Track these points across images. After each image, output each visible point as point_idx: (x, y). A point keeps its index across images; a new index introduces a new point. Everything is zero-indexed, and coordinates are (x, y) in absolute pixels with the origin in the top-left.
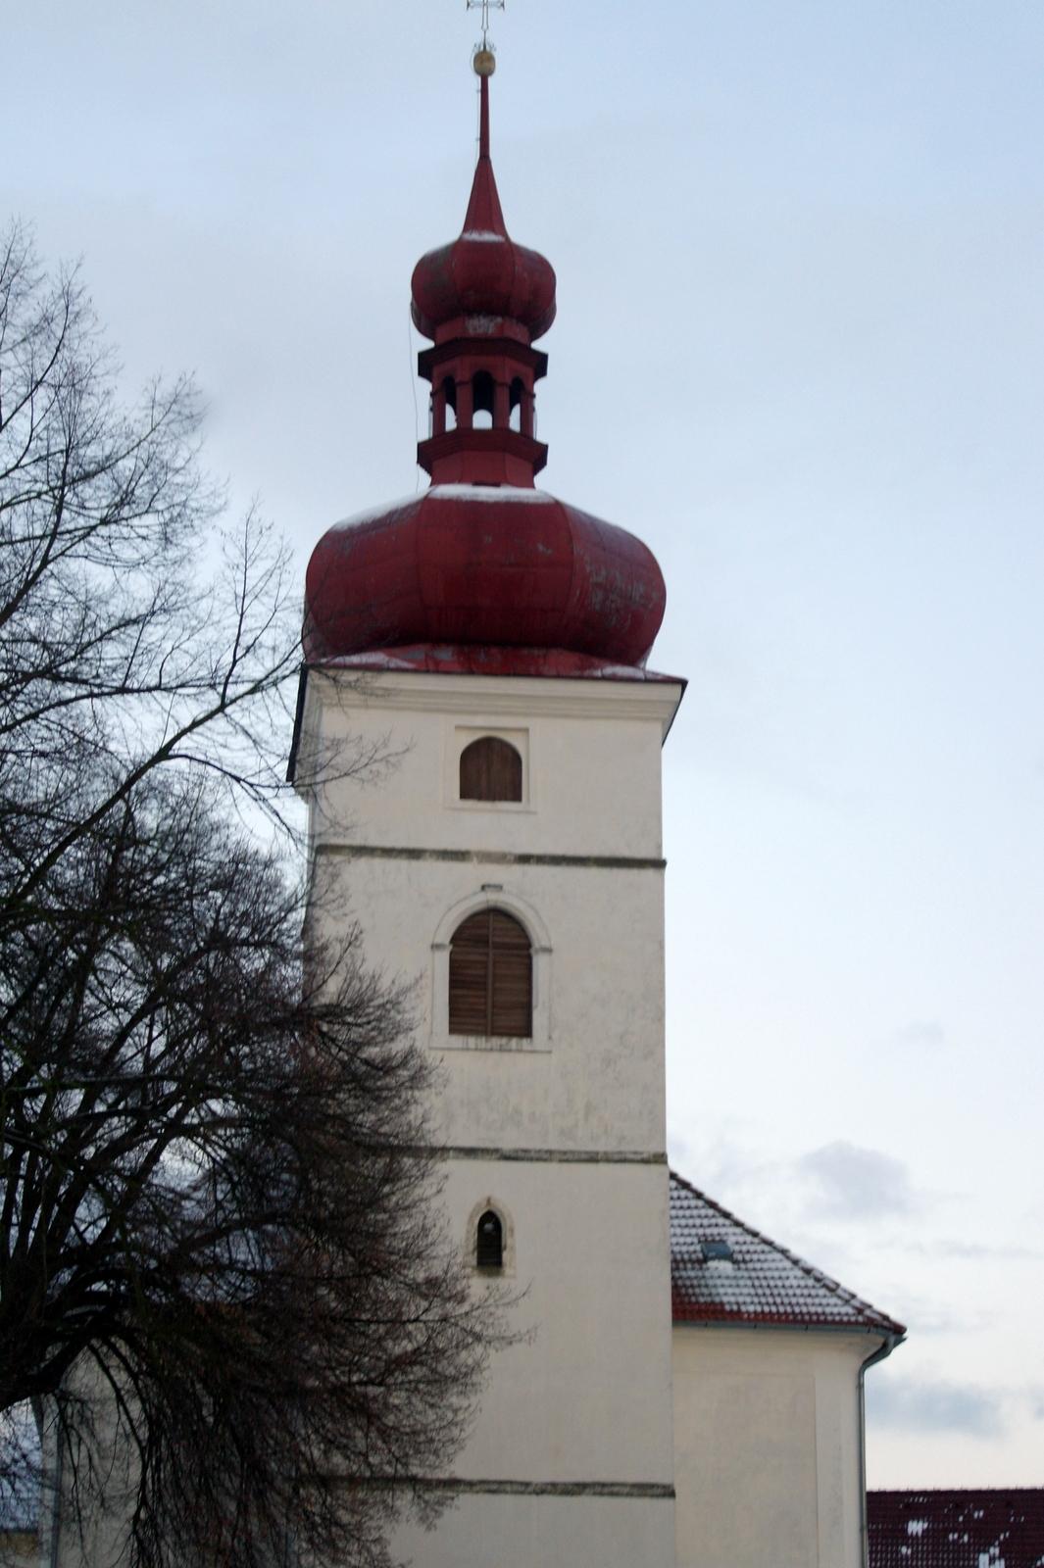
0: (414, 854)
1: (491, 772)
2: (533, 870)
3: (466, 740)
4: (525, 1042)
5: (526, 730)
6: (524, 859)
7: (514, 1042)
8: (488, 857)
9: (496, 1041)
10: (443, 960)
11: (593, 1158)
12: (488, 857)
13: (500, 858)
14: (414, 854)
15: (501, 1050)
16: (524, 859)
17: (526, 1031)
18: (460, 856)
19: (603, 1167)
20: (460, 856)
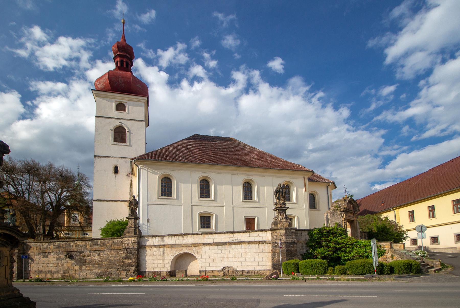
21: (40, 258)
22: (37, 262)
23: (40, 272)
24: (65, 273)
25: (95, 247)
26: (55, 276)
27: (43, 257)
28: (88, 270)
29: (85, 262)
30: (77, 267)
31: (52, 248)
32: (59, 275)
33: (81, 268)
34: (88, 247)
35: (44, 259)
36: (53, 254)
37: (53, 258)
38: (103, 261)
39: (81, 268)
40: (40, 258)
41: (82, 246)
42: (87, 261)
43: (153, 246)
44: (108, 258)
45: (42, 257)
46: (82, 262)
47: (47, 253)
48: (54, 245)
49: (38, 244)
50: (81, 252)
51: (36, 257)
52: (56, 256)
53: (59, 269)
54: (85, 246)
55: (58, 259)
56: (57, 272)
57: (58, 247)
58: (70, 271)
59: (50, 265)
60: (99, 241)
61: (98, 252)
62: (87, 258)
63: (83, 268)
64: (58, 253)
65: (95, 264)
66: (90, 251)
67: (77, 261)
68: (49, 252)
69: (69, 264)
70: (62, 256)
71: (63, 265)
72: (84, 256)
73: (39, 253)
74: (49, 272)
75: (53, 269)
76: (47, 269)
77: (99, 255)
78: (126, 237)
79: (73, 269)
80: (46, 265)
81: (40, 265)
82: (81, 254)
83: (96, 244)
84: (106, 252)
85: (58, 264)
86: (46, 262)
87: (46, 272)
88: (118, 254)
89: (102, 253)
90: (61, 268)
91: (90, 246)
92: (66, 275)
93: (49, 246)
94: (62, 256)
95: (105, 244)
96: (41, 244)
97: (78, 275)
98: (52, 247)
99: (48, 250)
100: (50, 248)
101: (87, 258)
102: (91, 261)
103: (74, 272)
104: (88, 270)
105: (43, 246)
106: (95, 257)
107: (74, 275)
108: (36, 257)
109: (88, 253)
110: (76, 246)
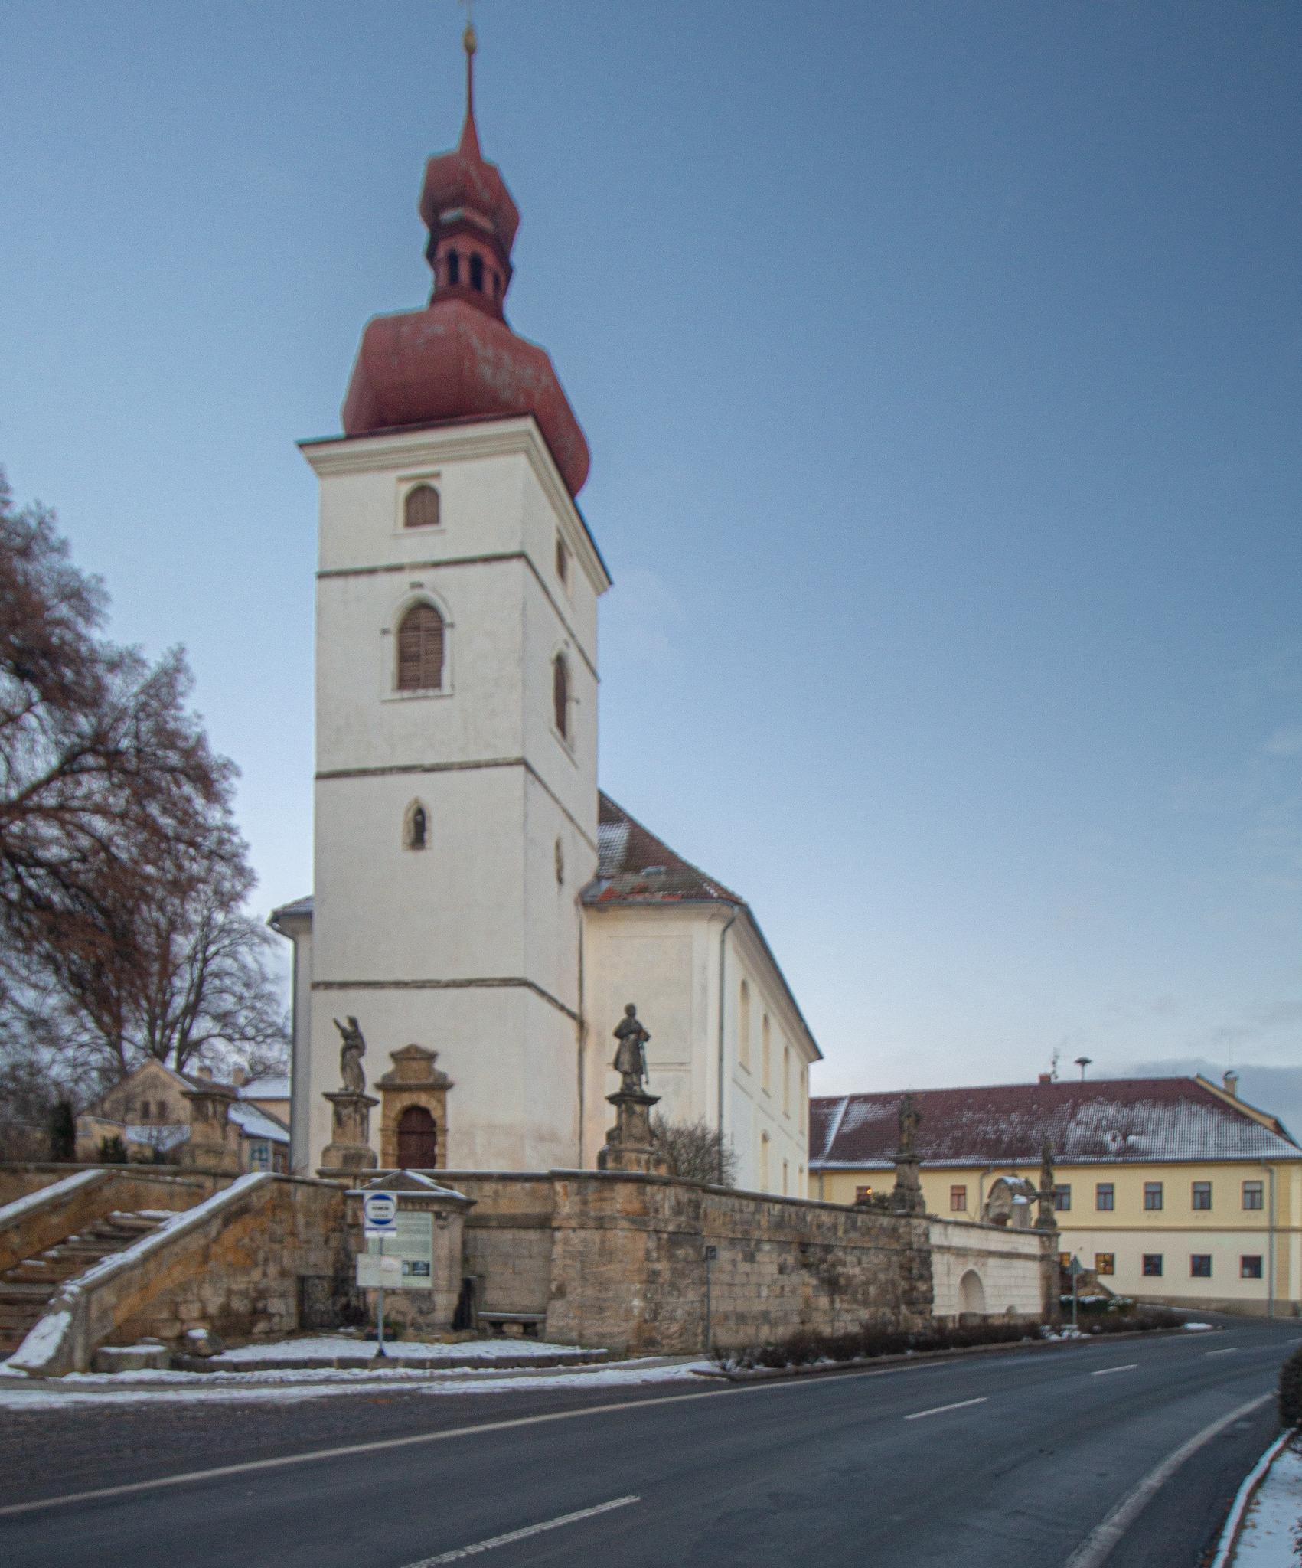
9: (421, 692)
10: (390, 643)
11: (478, 766)
15: (425, 698)
17: (438, 684)
19: (484, 772)
21: (734, 1262)
25: (854, 1235)
28: (847, 1311)
30: (823, 1301)
31: (764, 1223)
33: (832, 1302)
34: (840, 1233)
36: (767, 1247)
37: (768, 1261)
38: (866, 1283)
39: (832, 1302)
40: (734, 1262)
41: (829, 1229)
42: (842, 1281)
45: (740, 1256)
46: (833, 1285)
47: (753, 1243)
50: (828, 1249)
57: (780, 1224)
59: (765, 1292)
61: (857, 1252)
63: (838, 1305)
64: (783, 1246)
67: (822, 1281)
68: (759, 1241)
77: (859, 1263)
79: (817, 1309)
82: (830, 1257)
83: (854, 1227)
85: (782, 1288)
86: (754, 1279)
87: (755, 1318)
91: (846, 1232)
94: (790, 1259)
98: (764, 1223)
99: (757, 1234)
104: (847, 1311)
105: (741, 1211)
106: (852, 1270)
109: (841, 1254)
110: (819, 1227)
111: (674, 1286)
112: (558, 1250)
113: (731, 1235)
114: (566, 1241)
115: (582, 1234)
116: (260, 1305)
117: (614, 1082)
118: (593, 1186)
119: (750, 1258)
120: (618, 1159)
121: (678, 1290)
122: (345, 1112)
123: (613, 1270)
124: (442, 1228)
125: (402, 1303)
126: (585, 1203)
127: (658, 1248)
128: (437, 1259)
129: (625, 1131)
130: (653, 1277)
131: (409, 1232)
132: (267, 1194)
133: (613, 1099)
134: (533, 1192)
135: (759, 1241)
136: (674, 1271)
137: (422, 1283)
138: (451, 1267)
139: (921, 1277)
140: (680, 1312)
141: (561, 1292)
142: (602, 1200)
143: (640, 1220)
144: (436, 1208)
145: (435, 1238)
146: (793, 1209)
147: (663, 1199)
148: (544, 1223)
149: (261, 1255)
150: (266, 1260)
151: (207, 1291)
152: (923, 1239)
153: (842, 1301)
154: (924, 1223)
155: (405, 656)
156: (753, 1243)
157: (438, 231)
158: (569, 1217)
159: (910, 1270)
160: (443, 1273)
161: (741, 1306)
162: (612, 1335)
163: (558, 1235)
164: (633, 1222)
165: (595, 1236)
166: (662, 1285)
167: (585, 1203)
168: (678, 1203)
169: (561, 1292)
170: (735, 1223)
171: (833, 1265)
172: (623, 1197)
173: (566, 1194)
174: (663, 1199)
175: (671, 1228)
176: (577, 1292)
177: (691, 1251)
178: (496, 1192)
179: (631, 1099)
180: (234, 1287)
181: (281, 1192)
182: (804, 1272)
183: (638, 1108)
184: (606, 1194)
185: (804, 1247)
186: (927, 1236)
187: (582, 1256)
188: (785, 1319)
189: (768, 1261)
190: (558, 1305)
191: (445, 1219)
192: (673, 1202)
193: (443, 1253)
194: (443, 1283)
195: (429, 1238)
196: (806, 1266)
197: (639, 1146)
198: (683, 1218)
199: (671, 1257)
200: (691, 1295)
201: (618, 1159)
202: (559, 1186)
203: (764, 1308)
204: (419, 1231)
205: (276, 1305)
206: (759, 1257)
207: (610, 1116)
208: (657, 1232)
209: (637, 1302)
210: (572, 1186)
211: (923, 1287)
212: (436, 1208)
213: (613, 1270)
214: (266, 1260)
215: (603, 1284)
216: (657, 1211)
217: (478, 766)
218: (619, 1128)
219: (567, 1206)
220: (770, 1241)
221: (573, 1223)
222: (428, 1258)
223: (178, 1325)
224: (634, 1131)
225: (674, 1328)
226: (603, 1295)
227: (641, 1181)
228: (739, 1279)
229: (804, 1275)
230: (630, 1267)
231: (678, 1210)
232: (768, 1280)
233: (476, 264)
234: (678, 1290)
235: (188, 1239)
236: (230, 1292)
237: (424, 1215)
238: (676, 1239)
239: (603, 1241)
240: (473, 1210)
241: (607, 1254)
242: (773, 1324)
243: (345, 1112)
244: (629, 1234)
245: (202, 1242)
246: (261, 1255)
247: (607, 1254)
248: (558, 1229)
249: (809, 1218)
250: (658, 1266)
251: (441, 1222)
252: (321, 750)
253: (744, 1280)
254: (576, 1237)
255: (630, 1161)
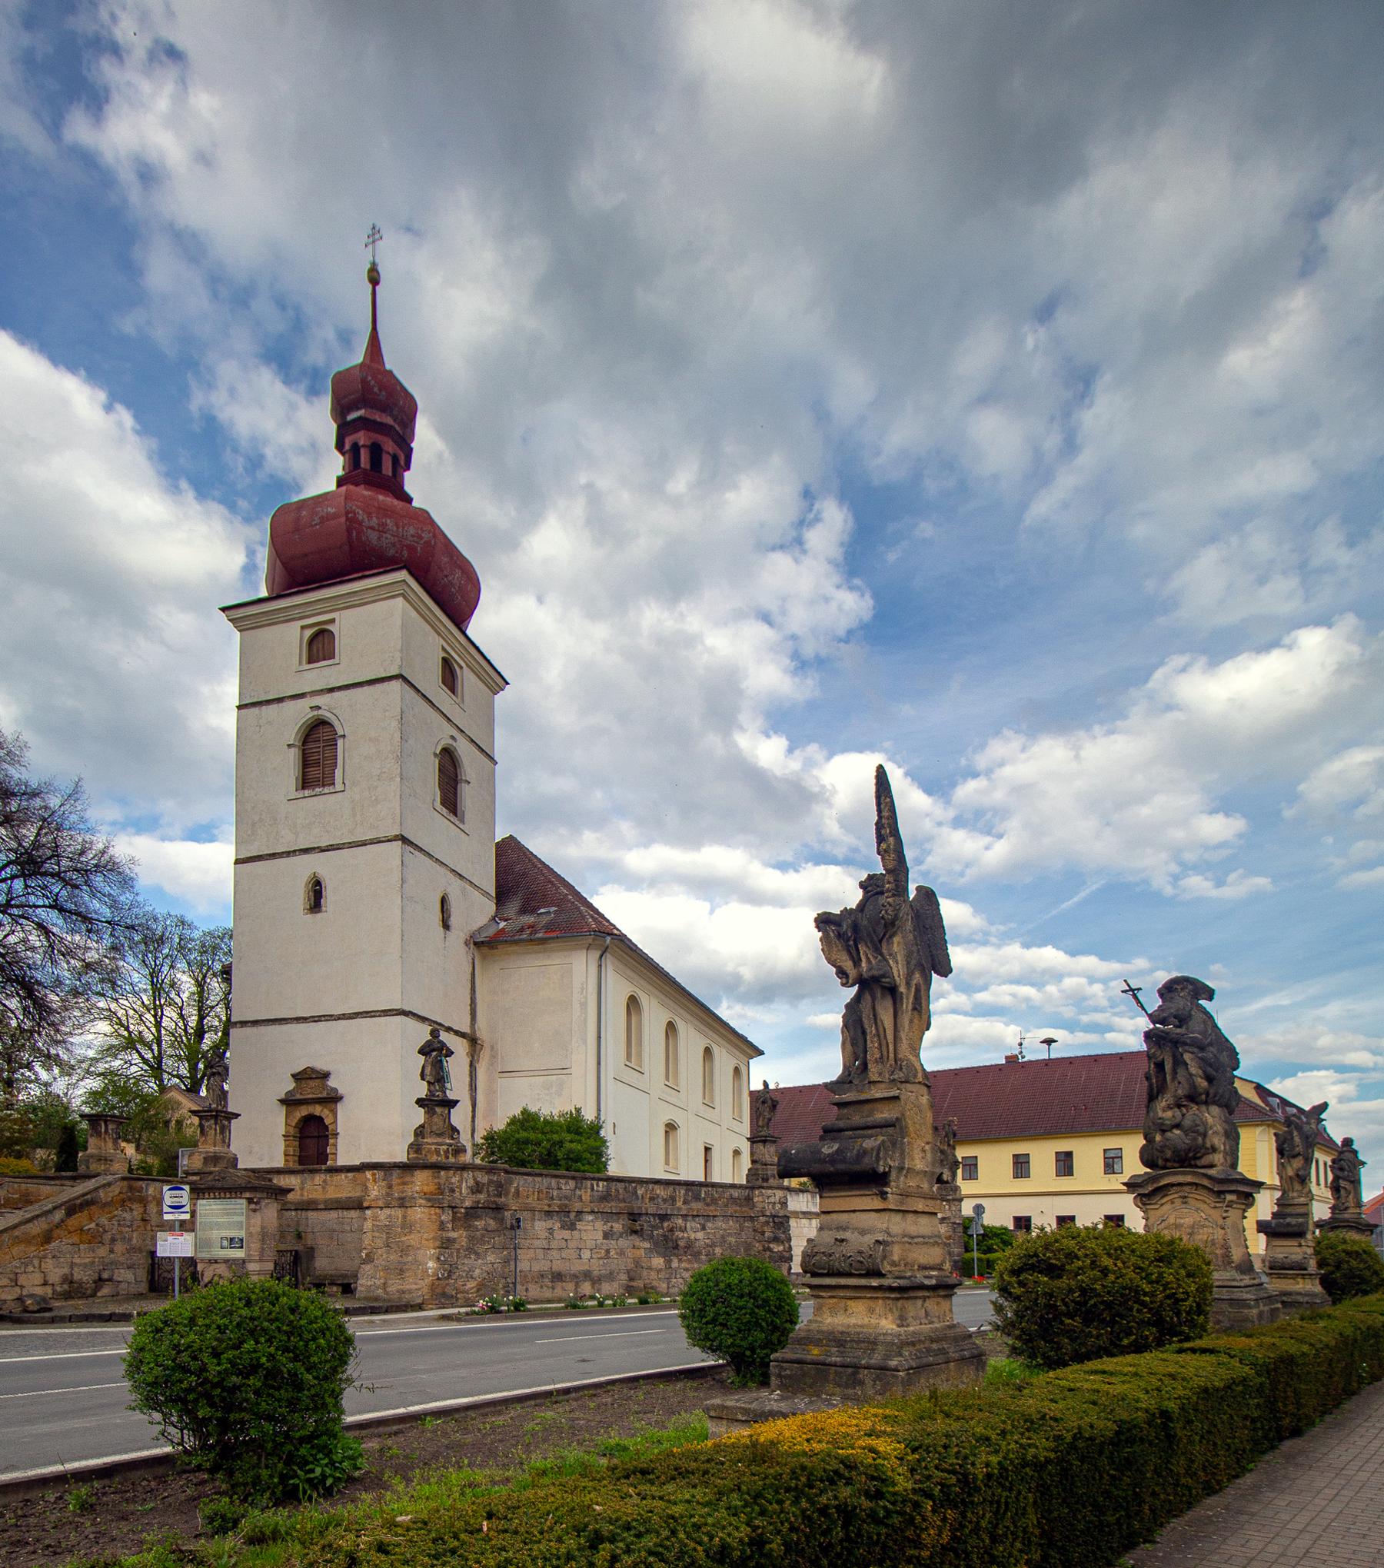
0: (280, 700)
1: (320, 645)
2: (336, 694)
3: (308, 633)
4: (331, 789)
5: (333, 621)
6: (331, 690)
7: (326, 790)
8: (314, 693)
9: (318, 790)
11: (364, 844)
12: (314, 693)
13: (322, 692)
14: (280, 700)
16: (331, 690)
18: (302, 696)
20: (302, 696)
21: (551, 1231)
22: (545, 1244)
23: (558, 1277)
24: (631, 1279)
25: (696, 1206)
26: (607, 1288)
27: (562, 1227)
29: (677, 1247)
30: (658, 1262)
31: (586, 1197)
32: (615, 1285)
33: (669, 1262)
34: (679, 1204)
35: (567, 1234)
36: (591, 1218)
37: (591, 1230)
38: (713, 1245)
40: (551, 1231)
41: (665, 1201)
42: (681, 1243)
43: (804, 1213)
44: (723, 1237)
46: (669, 1246)
47: (572, 1215)
48: (592, 1189)
49: (546, 1181)
50: (664, 1217)
51: (537, 1223)
52: (601, 1226)
53: (613, 1267)
54: (673, 1199)
55: (607, 1235)
56: (611, 1277)
57: (605, 1198)
58: (645, 1273)
59: (586, 1254)
60: (703, 1190)
62: (681, 1235)
63: (675, 1264)
64: (608, 1216)
65: (700, 1253)
66: (684, 1217)
67: (656, 1244)
68: (580, 1213)
69: (638, 1252)
70: (618, 1227)
71: (621, 1253)
72: (671, 1230)
73: (549, 1214)
74: (587, 1275)
75: (597, 1267)
76: (577, 1267)
77: (704, 1228)
78: (771, 1188)
79: (650, 1268)
80: (574, 1254)
81: (554, 1253)
82: (666, 1224)
83: (697, 1198)
84: (720, 1223)
85: (608, 1251)
86: (571, 1244)
87: (575, 1276)
88: (742, 1229)
89: (710, 1225)
90: (620, 1264)
91: (684, 1203)
92: (634, 1284)
93: (578, 1192)
94: (618, 1227)
95: (714, 1201)
96: (554, 1182)
97: (665, 1285)
98: (586, 1197)
99: (577, 1206)
100: (580, 1197)
101: (681, 1235)
102: (689, 1245)
103: (653, 1274)
105: (560, 1189)
106: (694, 1233)
107: (655, 1283)
108: (537, 1223)
109: (680, 1221)
110: (652, 1199)
111: (470, 1250)
112: (368, 1225)
113: (546, 1208)
114: (375, 1218)
115: (388, 1211)
116: (105, 1276)
117: (422, 1090)
118: (396, 1173)
119: (572, 1227)
120: (418, 1151)
121: (477, 1254)
122: (207, 1124)
123: (413, 1239)
124: (255, 1211)
125: (221, 1269)
126: (390, 1187)
127: (453, 1220)
128: (250, 1234)
129: (427, 1130)
130: (446, 1244)
131: (228, 1214)
132: (115, 1190)
133: (420, 1102)
134: (354, 1179)
135: (580, 1213)
136: (471, 1239)
137: (239, 1254)
138: (263, 1241)
139: (776, 1240)
140: (478, 1271)
141: (369, 1259)
142: (404, 1184)
143: (434, 1200)
144: (248, 1195)
145: (248, 1218)
146: (621, 1186)
147: (460, 1181)
148: (358, 1205)
149: (107, 1237)
150: (113, 1240)
151: (49, 1264)
152: (778, 1207)
153: (680, 1261)
154: (779, 1193)
155: (306, 763)
156: (572, 1215)
157: (344, 429)
158: (376, 1199)
159: (763, 1233)
160: (256, 1246)
161: (557, 1266)
162: (410, 1291)
163: (368, 1212)
164: (429, 1200)
165: (399, 1213)
166: (458, 1250)
167: (390, 1187)
168: (477, 1183)
169: (369, 1259)
170: (552, 1198)
171: (671, 1230)
172: (421, 1181)
173: (374, 1180)
174: (460, 1181)
175: (467, 1204)
176: (382, 1257)
177: (491, 1222)
178: (325, 1181)
179: (436, 1103)
180: (77, 1261)
181: (131, 1188)
182: (634, 1237)
183: (438, 1110)
184: (407, 1179)
185: (634, 1216)
186: (784, 1204)
187: (388, 1229)
188: (611, 1277)
189: (591, 1230)
190: (367, 1267)
191: (256, 1203)
192: (471, 1182)
193: (257, 1229)
194: (255, 1254)
195: (243, 1219)
196: (635, 1232)
197: (440, 1140)
198: (482, 1197)
199: (468, 1228)
200: (490, 1258)
201: (418, 1151)
202: (369, 1174)
203: (586, 1267)
204: (235, 1214)
205: (124, 1275)
206: (579, 1225)
207: (419, 1116)
208: (453, 1208)
209: (431, 1264)
210: (379, 1174)
211: (777, 1248)
212: (248, 1195)
213: (413, 1239)
214: (113, 1240)
215: (405, 1250)
216: (452, 1191)
217: (364, 844)
218: (422, 1126)
219: (375, 1190)
220: (593, 1212)
221: (380, 1204)
222: (242, 1234)
223: (18, 1289)
224: (434, 1128)
225: (471, 1284)
226: (405, 1259)
227: (436, 1167)
228: (554, 1244)
229: (636, 1240)
230: (425, 1236)
231: (477, 1188)
232: (590, 1244)
233: (376, 451)
234: (477, 1254)
235: (30, 1225)
236: (72, 1265)
237: (239, 1201)
238: (473, 1212)
239: (404, 1217)
240: (290, 1196)
241: (408, 1227)
242: (596, 1281)
243: (207, 1124)
244: (426, 1210)
245: (45, 1226)
246: (107, 1237)
247: (408, 1227)
248: (368, 1208)
249: (639, 1192)
250: (453, 1235)
251: (253, 1206)
252: (239, 843)
253: (564, 1244)
254: (383, 1215)
255: (429, 1151)
